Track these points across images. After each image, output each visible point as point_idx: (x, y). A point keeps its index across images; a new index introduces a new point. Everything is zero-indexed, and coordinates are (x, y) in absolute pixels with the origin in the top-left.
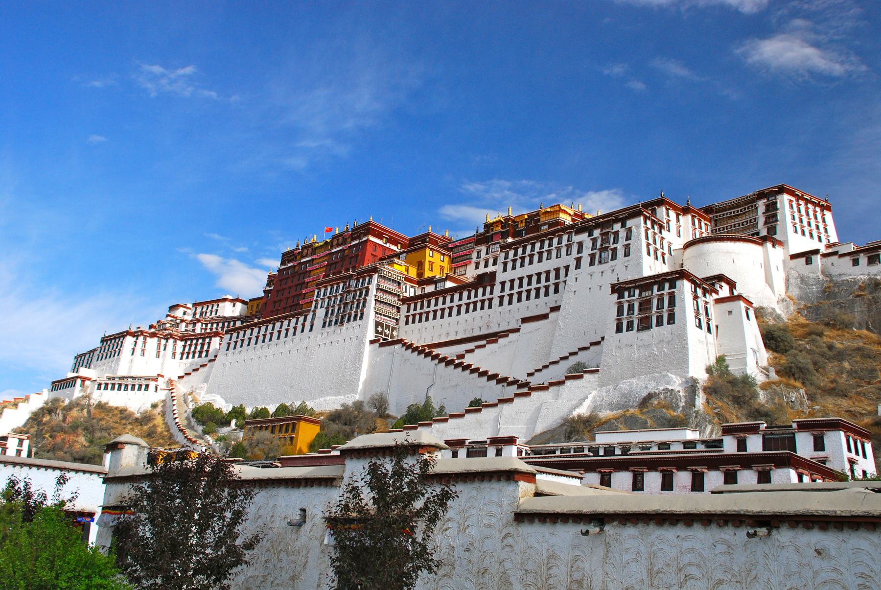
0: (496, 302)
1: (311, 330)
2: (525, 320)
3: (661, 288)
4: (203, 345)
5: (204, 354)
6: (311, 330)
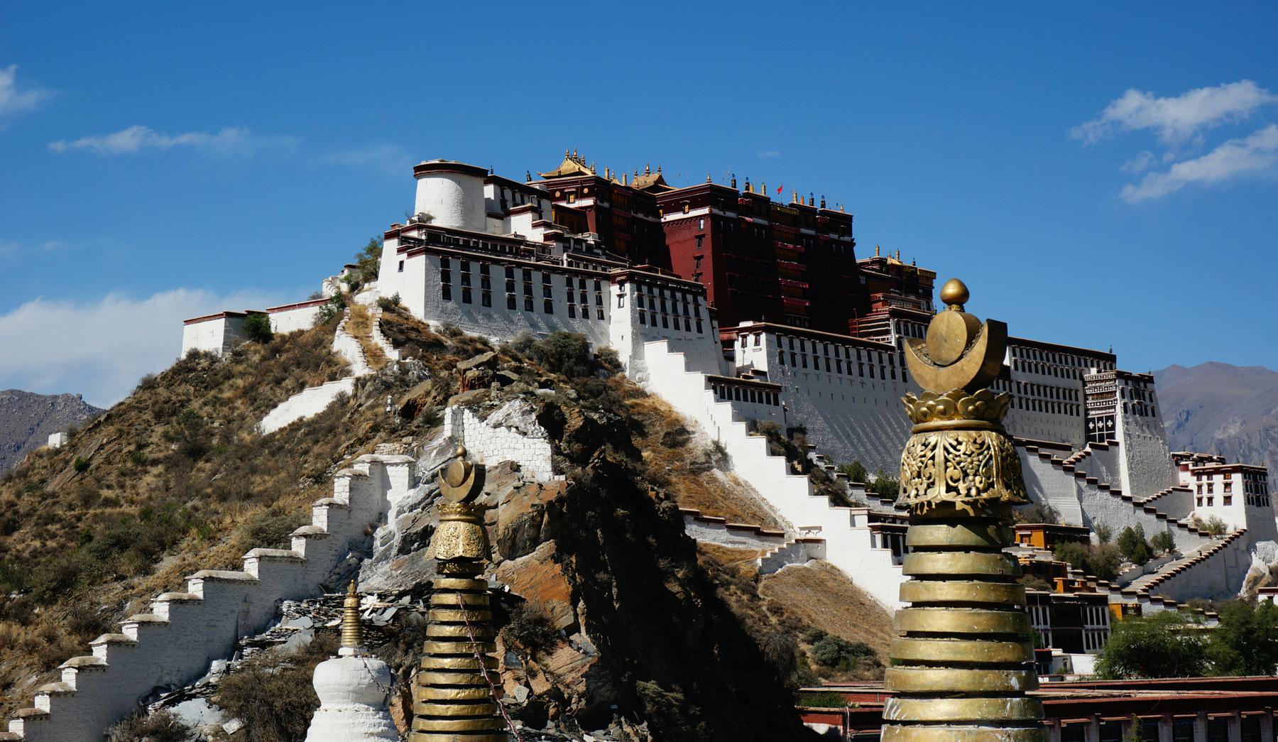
0: (1016, 401)
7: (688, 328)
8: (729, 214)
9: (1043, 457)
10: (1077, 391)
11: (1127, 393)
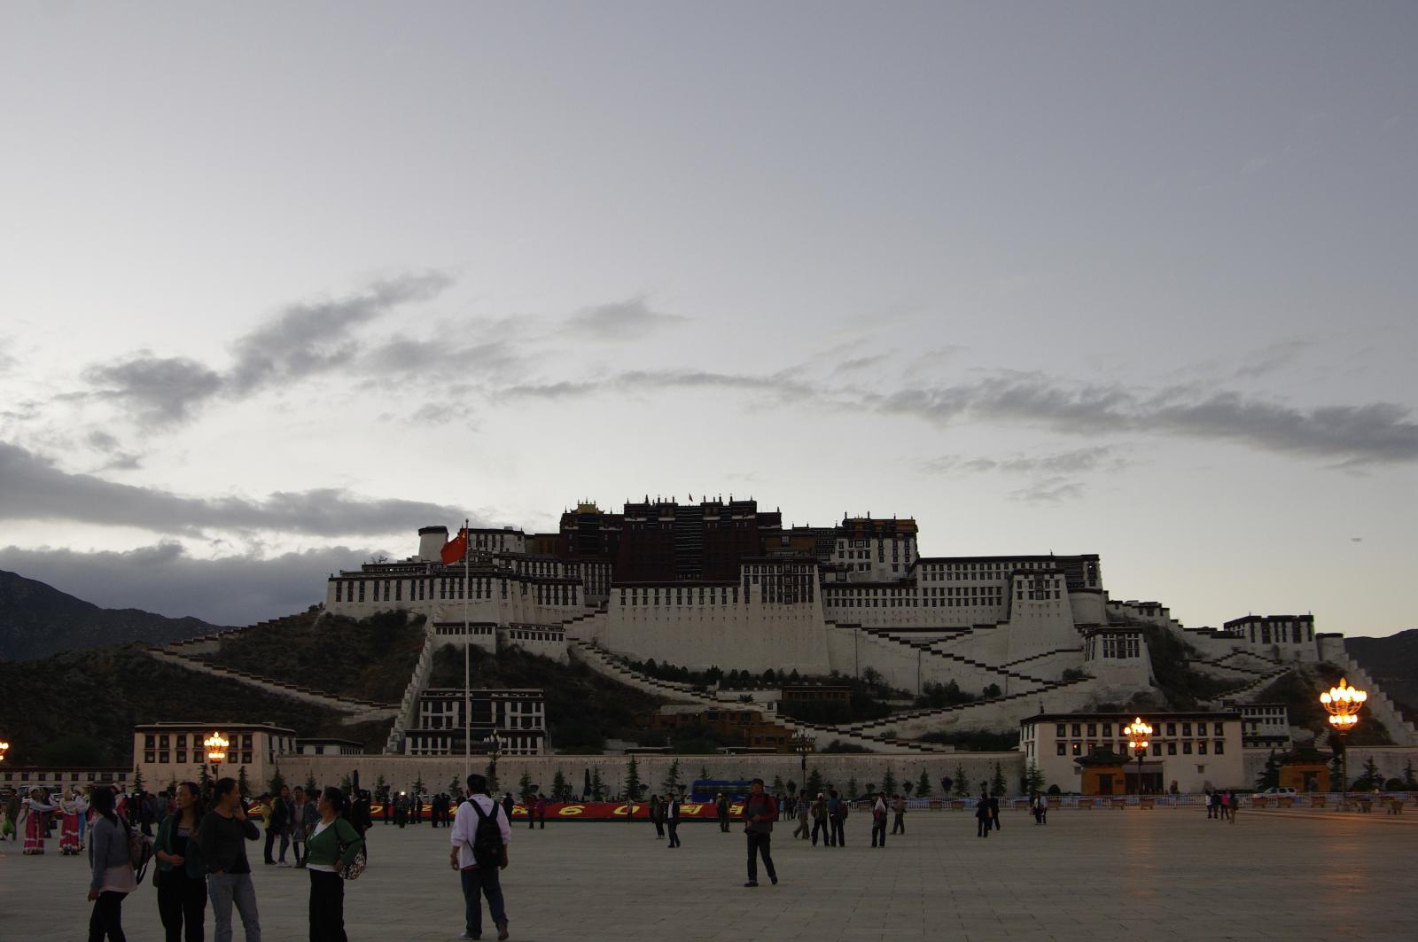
0: (920, 602)
1: (747, 601)
2: (976, 626)
3: (1129, 636)
4: (565, 590)
5: (570, 601)
6: (747, 601)
7: (479, 597)
8: (639, 520)
9: (892, 639)
10: (999, 589)
11: (1025, 583)
